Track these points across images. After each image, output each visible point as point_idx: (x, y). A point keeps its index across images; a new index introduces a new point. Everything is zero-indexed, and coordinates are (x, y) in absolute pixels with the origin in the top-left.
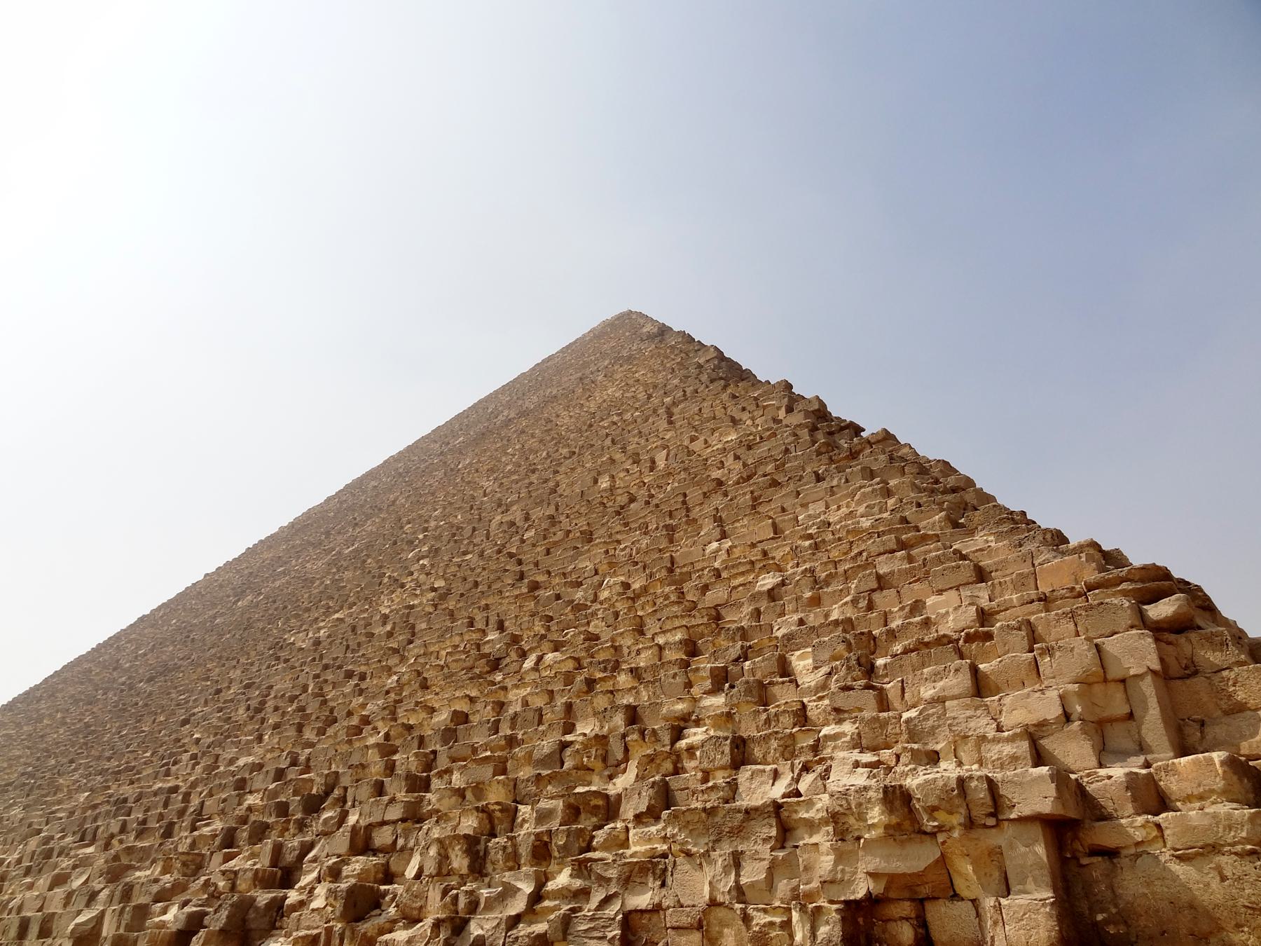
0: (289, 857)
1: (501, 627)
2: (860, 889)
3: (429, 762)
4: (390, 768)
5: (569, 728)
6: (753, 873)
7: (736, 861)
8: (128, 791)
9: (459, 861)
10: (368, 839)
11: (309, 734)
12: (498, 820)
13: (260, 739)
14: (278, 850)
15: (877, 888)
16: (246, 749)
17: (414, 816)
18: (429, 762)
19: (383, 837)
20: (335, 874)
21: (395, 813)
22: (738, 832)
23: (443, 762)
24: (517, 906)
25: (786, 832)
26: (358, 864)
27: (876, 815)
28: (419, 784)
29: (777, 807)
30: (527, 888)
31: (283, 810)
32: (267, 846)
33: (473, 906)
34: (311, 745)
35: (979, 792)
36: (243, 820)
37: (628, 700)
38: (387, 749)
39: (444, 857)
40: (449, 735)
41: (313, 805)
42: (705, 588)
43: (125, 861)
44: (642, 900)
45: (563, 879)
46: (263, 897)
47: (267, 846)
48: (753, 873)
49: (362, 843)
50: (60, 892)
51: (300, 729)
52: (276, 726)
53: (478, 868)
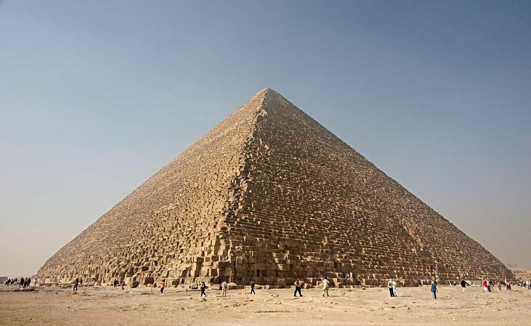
1: (178, 220)
4: (154, 247)
5: (172, 244)
8: (122, 246)
10: (148, 259)
15: (185, 269)
19: (150, 259)
20: (143, 264)
21: (151, 256)
23: (160, 248)
24: (158, 270)
25: (182, 262)
30: (159, 268)
32: (137, 260)
34: (147, 241)
36: (136, 255)
38: (155, 244)
41: (144, 253)
43: (120, 260)
46: (135, 267)
47: (137, 260)
50: (111, 265)
52: (145, 236)
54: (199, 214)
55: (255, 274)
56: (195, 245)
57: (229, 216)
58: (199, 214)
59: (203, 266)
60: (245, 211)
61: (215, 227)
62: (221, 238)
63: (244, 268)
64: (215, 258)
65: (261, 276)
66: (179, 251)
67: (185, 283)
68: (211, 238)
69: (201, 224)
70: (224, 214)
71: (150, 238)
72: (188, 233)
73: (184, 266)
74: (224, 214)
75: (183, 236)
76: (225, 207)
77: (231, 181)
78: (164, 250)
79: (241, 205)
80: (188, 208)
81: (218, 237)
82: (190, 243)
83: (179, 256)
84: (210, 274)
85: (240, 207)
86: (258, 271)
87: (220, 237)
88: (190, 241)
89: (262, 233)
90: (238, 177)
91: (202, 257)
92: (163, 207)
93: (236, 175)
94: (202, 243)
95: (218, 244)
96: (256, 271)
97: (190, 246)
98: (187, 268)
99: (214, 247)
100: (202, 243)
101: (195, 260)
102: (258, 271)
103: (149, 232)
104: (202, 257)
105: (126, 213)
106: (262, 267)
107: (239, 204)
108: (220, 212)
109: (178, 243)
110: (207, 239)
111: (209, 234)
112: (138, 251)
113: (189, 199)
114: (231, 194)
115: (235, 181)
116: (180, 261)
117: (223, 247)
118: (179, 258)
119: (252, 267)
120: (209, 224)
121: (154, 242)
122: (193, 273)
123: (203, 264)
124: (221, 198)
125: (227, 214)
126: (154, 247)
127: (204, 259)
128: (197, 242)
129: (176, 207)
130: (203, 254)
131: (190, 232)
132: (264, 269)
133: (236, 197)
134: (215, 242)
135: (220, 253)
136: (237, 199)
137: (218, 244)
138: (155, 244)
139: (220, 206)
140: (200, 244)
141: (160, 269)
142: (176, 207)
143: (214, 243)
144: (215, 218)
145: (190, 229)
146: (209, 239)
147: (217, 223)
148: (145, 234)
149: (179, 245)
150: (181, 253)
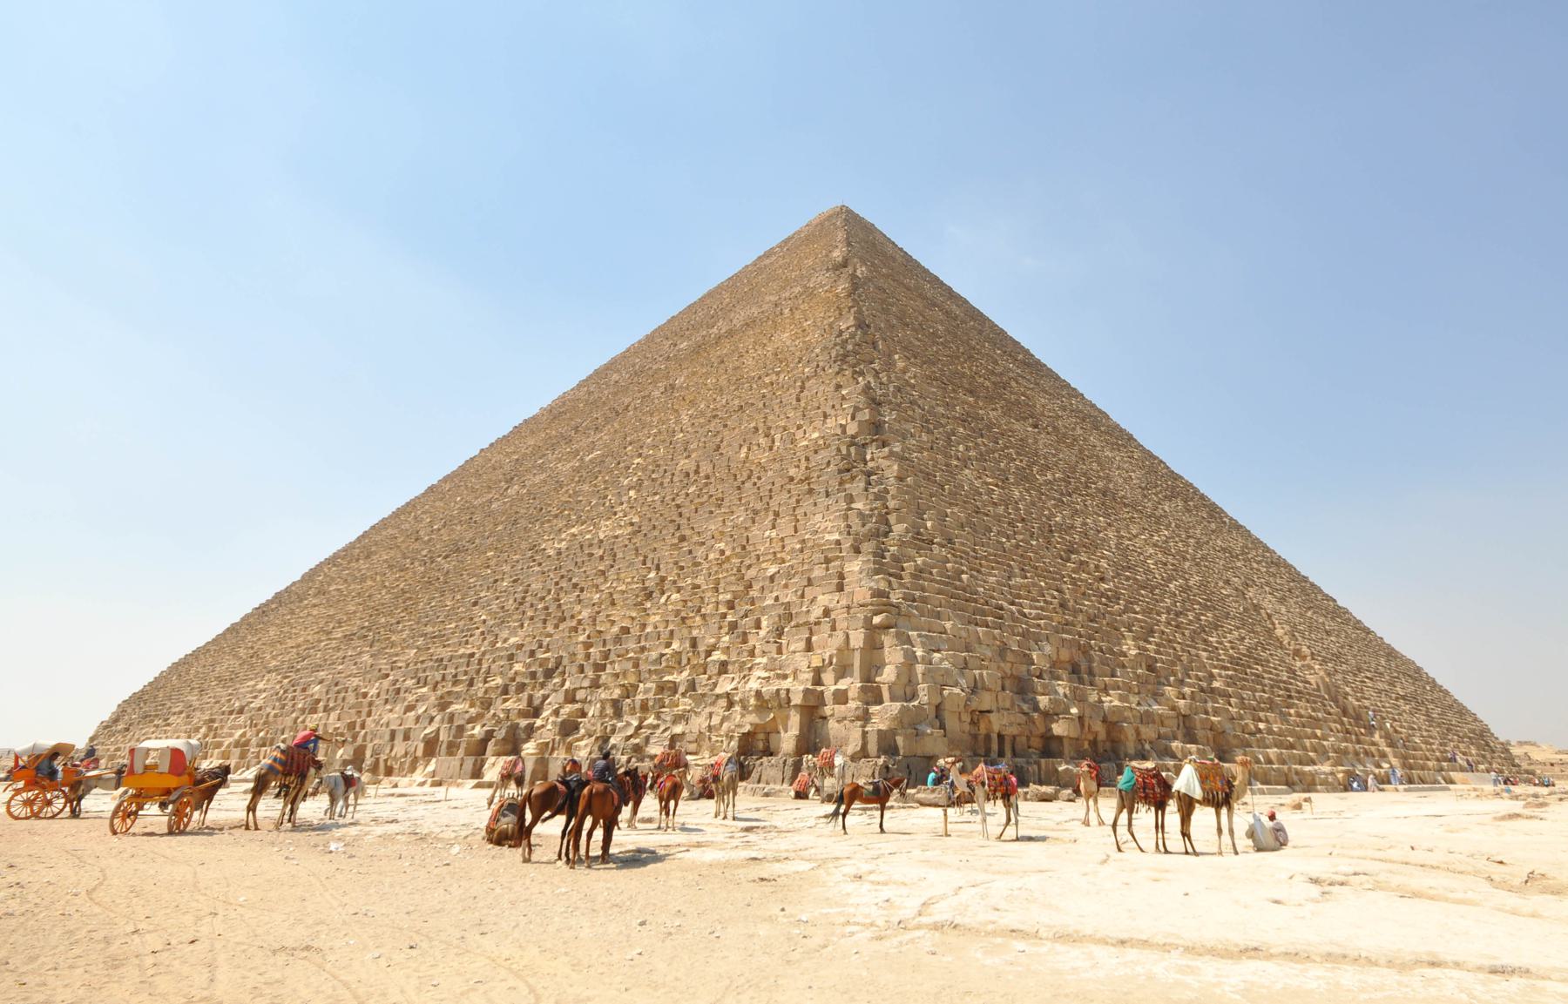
0: (536, 702)
2: (747, 728)
3: (606, 655)
4: (588, 656)
5: (668, 645)
6: (716, 720)
7: (711, 715)
8: (444, 653)
9: (609, 711)
11: (550, 629)
12: (629, 691)
13: (522, 626)
14: (531, 697)
16: (514, 633)
17: (595, 684)
18: (606, 655)
19: (580, 695)
21: (586, 683)
22: (713, 704)
23: (612, 657)
25: (731, 704)
26: (568, 708)
27: (752, 701)
28: (600, 668)
29: (728, 694)
31: (533, 675)
33: (613, 731)
34: (550, 635)
35: (783, 694)
36: (513, 679)
37: (695, 633)
38: (588, 645)
39: (603, 708)
40: (618, 640)
41: (549, 674)
42: (749, 567)
44: (678, 729)
45: (651, 720)
48: (716, 720)
49: (570, 698)
51: (545, 622)
52: (532, 618)
53: (618, 714)
54: (744, 548)
55: (995, 746)
56: (774, 647)
57: (880, 554)
58: (744, 548)
59: (825, 718)
60: (921, 541)
61: (840, 588)
62: (885, 627)
63: (967, 727)
64: (872, 695)
65: (1008, 753)
66: (713, 670)
67: (755, 775)
68: (841, 625)
69: (772, 579)
70: (857, 551)
71: (556, 626)
72: (723, 610)
73: (745, 721)
74: (857, 551)
75: (704, 616)
76: (849, 526)
77: (839, 450)
78: (636, 665)
79: (899, 522)
80: (688, 532)
81: (868, 620)
82: (745, 641)
83: (715, 685)
84: (872, 747)
85: (899, 529)
86: (1001, 737)
87: (877, 620)
88: (745, 634)
89: (984, 613)
90: (853, 437)
91: (819, 688)
92: (574, 530)
93: (844, 432)
94: (809, 641)
95: (873, 646)
96: (994, 737)
97: (752, 653)
98: (756, 726)
99: (857, 655)
100: (809, 641)
101: (797, 699)
102: (1001, 737)
103: (546, 608)
104: (819, 688)
105: (418, 552)
106: (1011, 724)
107: (892, 518)
108: (838, 542)
109: (694, 643)
110: (826, 627)
111: (827, 612)
112: (518, 667)
113: (678, 506)
114: (857, 487)
115: (853, 449)
116: (723, 702)
117: (893, 656)
118: (718, 691)
119: (982, 726)
120: (809, 580)
121: (582, 638)
122: (787, 740)
123: (827, 710)
124: (822, 500)
125: (868, 547)
126: (588, 656)
127: (828, 696)
128: (780, 636)
129: (630, 529)
130: (818, 681)
131: (731, 605)
132: (1014, 730)
133: (878, 497)
134: (862, 636)
135: (888, 675)
136: (878, 504)
137: (873, 646)
138: (588, 645)
139: (827, 526)
140: (802, 645)
141: (639, 727)
142: (630, 529)
143: (858, 639)
144: (828, 561)
145: (729, 597)
146: (833, 629)
147: (841, 576)
148: (530, 614)
149: (702, 648)
150: (720, 673)
